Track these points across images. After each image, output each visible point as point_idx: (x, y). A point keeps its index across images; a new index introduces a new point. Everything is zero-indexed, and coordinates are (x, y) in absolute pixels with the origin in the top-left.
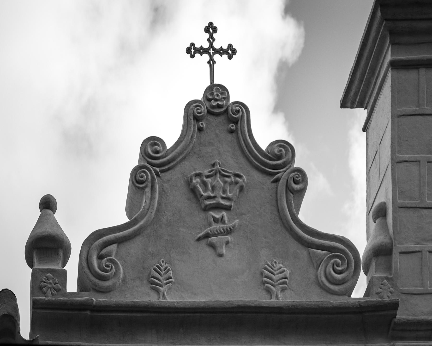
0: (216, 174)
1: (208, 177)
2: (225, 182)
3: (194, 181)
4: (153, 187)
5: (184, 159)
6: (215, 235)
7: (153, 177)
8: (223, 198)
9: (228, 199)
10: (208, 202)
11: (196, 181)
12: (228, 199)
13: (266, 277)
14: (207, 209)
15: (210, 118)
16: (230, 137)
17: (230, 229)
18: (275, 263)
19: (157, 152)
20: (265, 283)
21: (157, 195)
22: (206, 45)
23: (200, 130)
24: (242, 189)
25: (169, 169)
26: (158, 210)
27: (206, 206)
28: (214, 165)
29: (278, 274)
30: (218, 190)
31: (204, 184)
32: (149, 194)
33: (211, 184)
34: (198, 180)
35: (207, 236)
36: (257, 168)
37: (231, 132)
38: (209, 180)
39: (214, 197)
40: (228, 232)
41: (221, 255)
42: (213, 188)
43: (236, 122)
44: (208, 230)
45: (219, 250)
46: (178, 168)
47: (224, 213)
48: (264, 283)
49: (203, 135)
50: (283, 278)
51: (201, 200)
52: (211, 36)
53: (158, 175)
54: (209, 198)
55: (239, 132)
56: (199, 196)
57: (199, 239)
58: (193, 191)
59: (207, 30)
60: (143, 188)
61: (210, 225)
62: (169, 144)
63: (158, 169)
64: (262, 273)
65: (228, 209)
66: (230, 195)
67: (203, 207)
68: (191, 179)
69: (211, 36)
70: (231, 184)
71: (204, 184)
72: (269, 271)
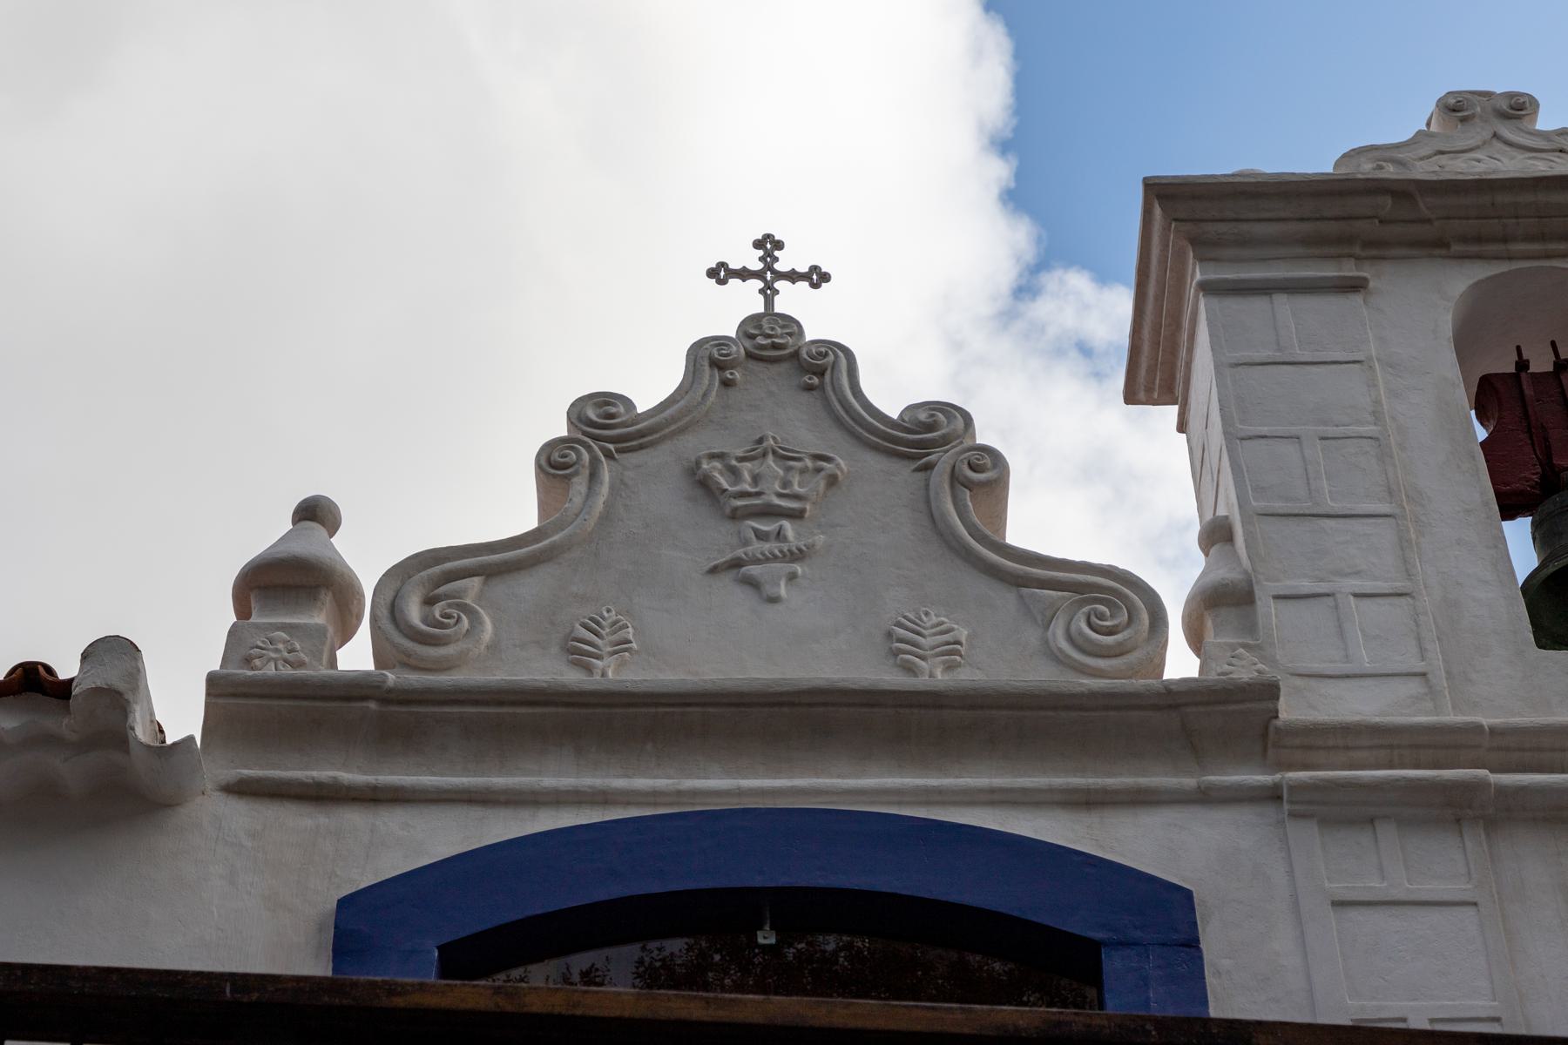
0: (764, 455)
1: (742, 459)
2: (788, 469)
3: (705, 466)
4: (594, 476)
5: (682, 431)
6: (757, 561)
7: (595, 461)
8: (780, 495)
9: (797, 497)
10: (739, 503)
11: (714, 469)
12: (797, 497)
13: (901, 641)
14: (735, 516)
15: (753, 365)
16: (805, 397)
17: (800, 550)
18: (927, 614)
19: (612, 416)
20: (896, 646)
21: (605, 490)
22: (758, 266)
23: (727, 384)
24: (832, 481)
25: (641, 447)
26: (606, 517)
27: (735, 509)
28: (760, 441)
29: (935, 634)
30: (772, 480)
31: (734, 473)
32: (583, 489)
33: (750, 471)
34: (717, 464)
35: (736, 564)
36: (875, 448)
37: (809, 388)
38: (748, 465)
39: (758, 494)
40: (797, 556)
41: (774, 600)
42: (756, 479)
43: (821, 373)
44: (740, 552)
45: (769, 590)
46: (666, 447)
47: (787, 525)
48: (896, 653)
49: (731, 391)
50: (948, 643)
51: (722, 499)
52: (769, 254)
53: (609, 455)
54: (743, 495)
55: (829, 388)
56: (717, 493)
57: (714, 570)
58: (704, 485)
59: (758, 244)
60: (568, 477)
61: (746, 543)
62: (642, 407)
63: (611, 447)
64: (889, 635)
65: (796, 515)
66: (796, 488)
67: (728, 511)
68: (698, 464)
69: (769, 254)
70: (803, 471)
71: (734, 473)
72: (907, 629)
